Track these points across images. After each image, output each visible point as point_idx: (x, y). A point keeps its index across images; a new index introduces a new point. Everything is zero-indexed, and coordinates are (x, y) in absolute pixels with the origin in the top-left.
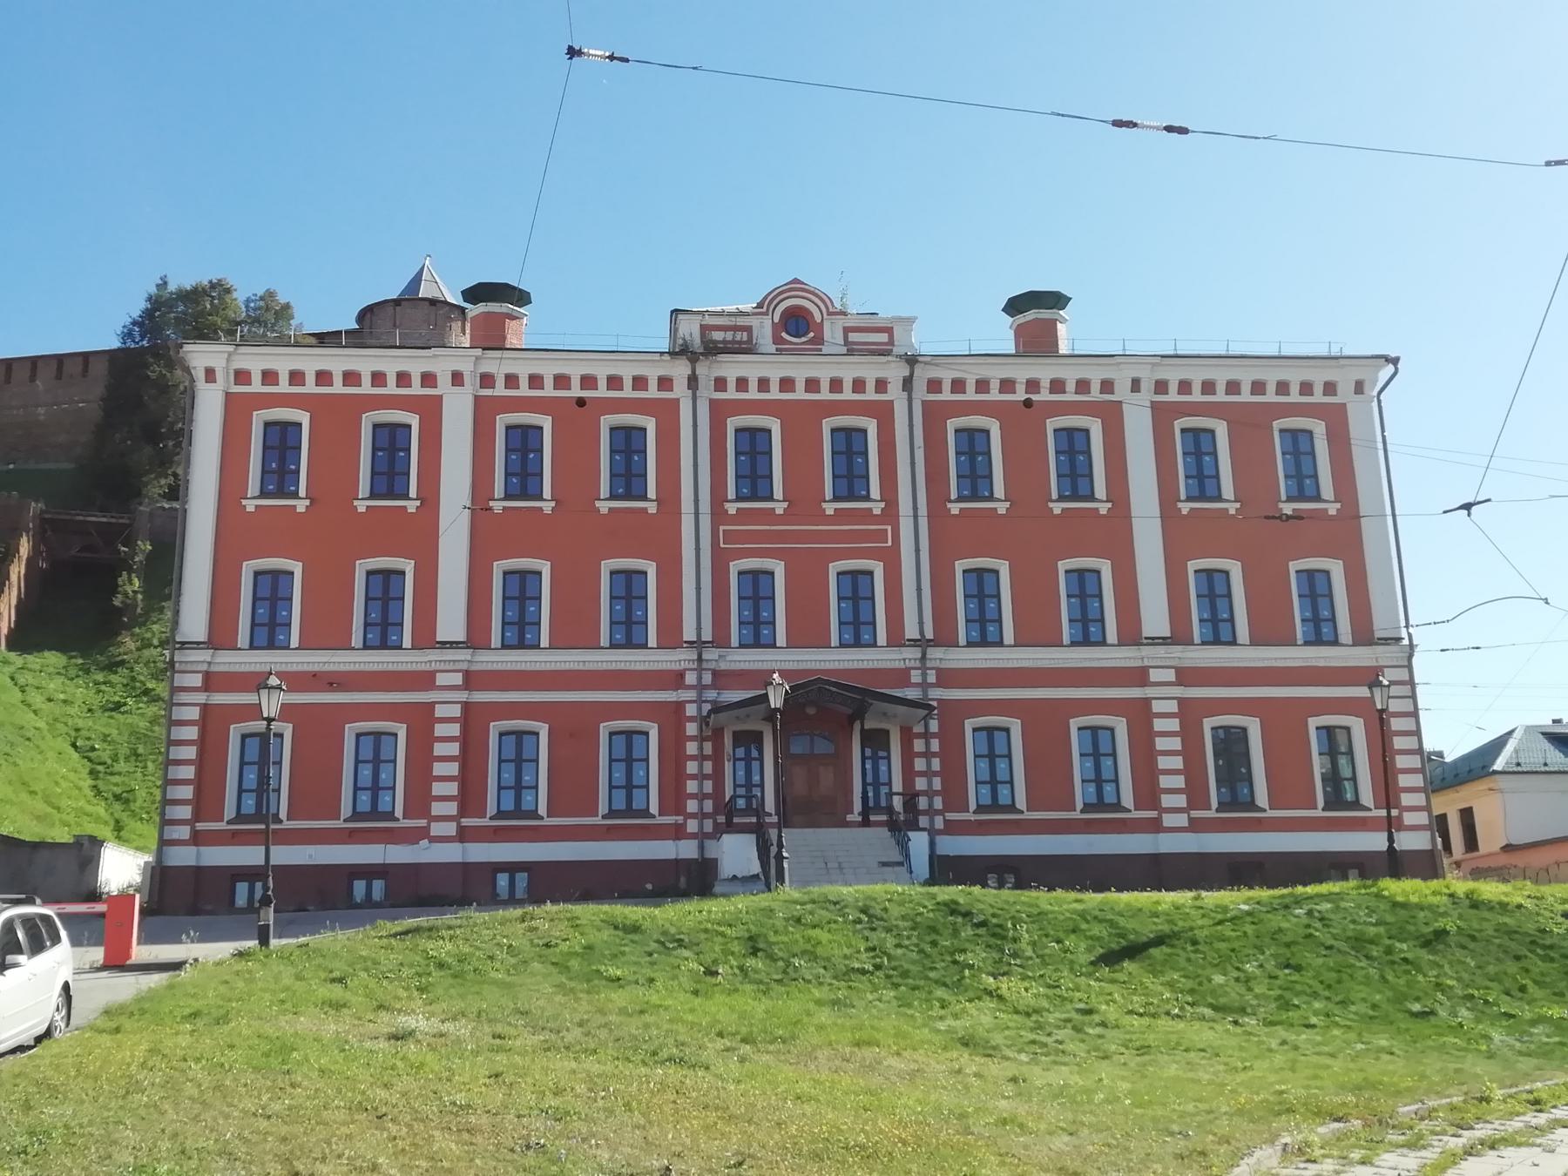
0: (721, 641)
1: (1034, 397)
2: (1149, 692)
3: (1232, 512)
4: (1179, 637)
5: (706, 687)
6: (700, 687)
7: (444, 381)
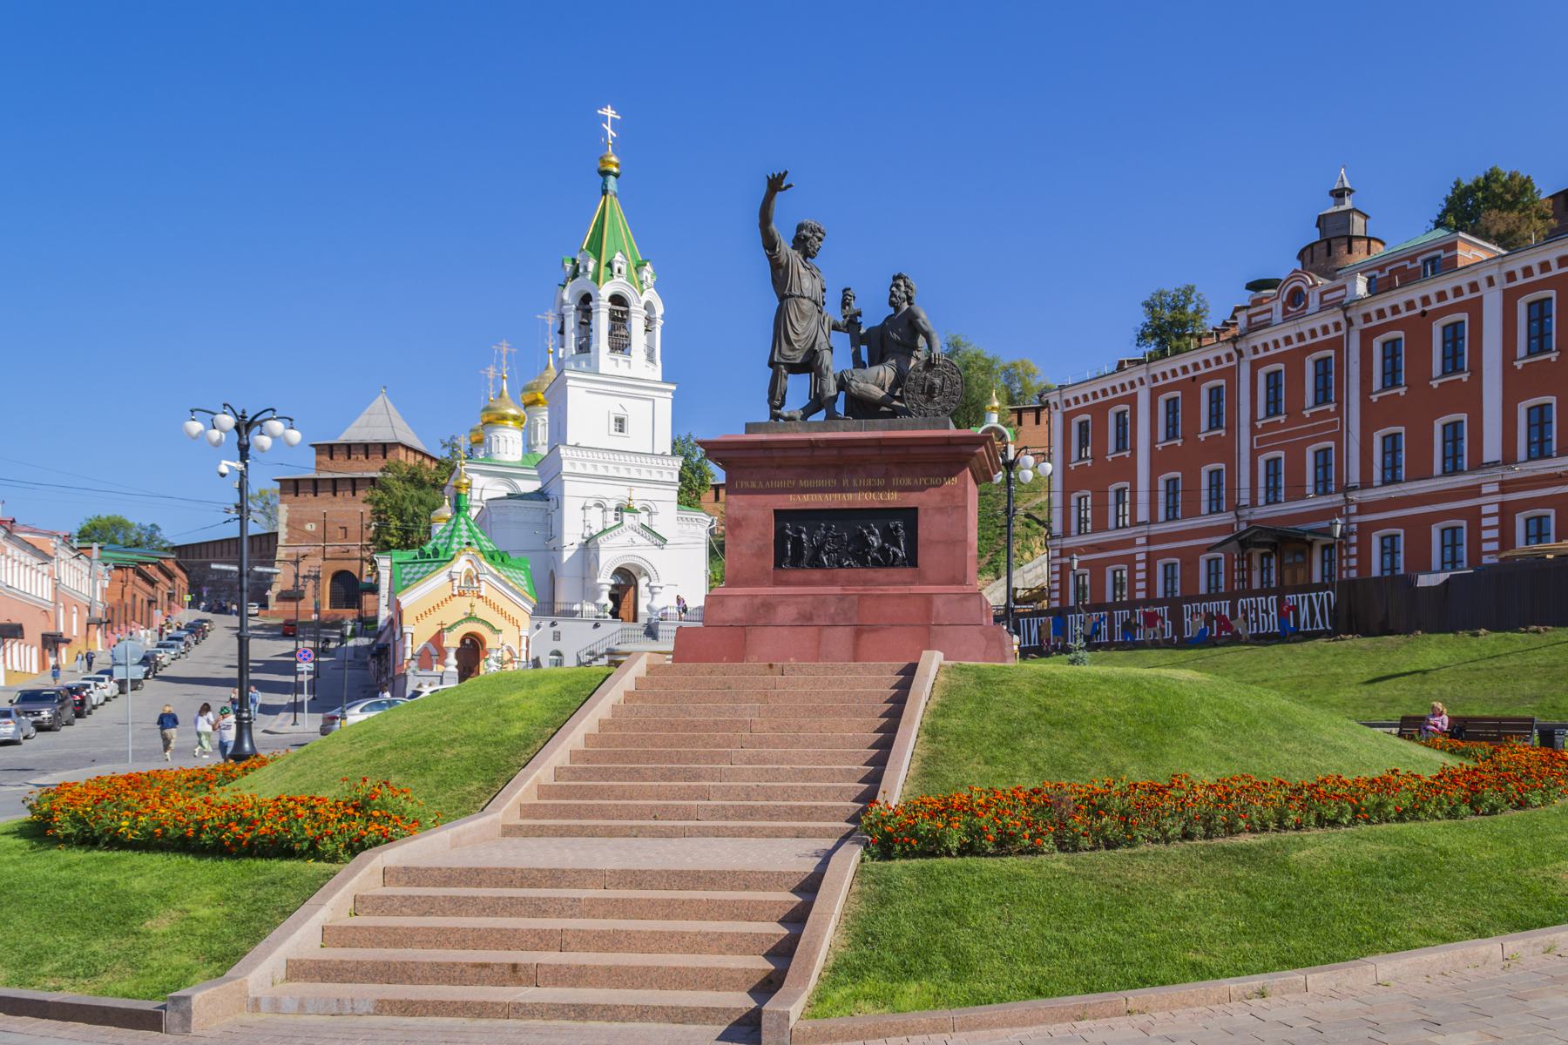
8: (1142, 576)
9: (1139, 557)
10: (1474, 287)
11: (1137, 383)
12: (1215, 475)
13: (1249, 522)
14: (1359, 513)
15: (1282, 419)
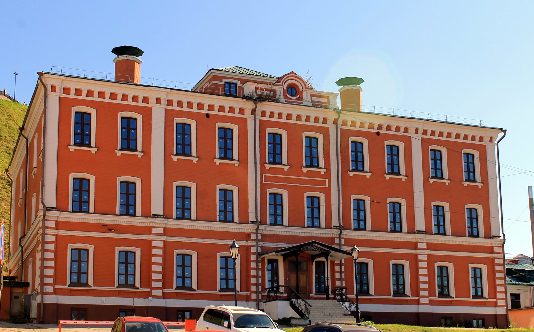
0: (263, 222)
1: (381, 132)
2: (418, 252)
3: (447, 184)
5: (259, 241)
6: (256, 240)
7: (152, 101)
10: (406, 130)
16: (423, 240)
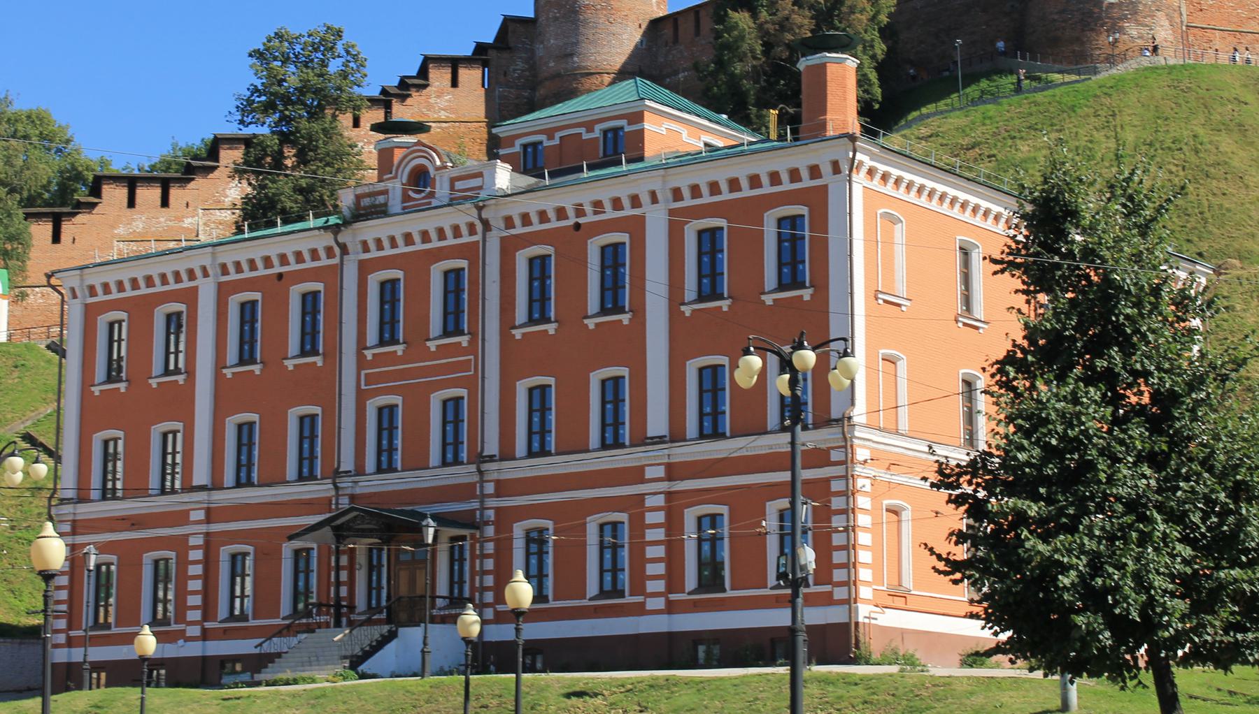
1: (581, 220)
4: (676, 435)
8: (196, 570)
9: (193, 541)
11: (198, 273)
12: (308, 423)
13: (353, 498)
14: (498, 494)
15: (399, 349)
16: (653, 460)
